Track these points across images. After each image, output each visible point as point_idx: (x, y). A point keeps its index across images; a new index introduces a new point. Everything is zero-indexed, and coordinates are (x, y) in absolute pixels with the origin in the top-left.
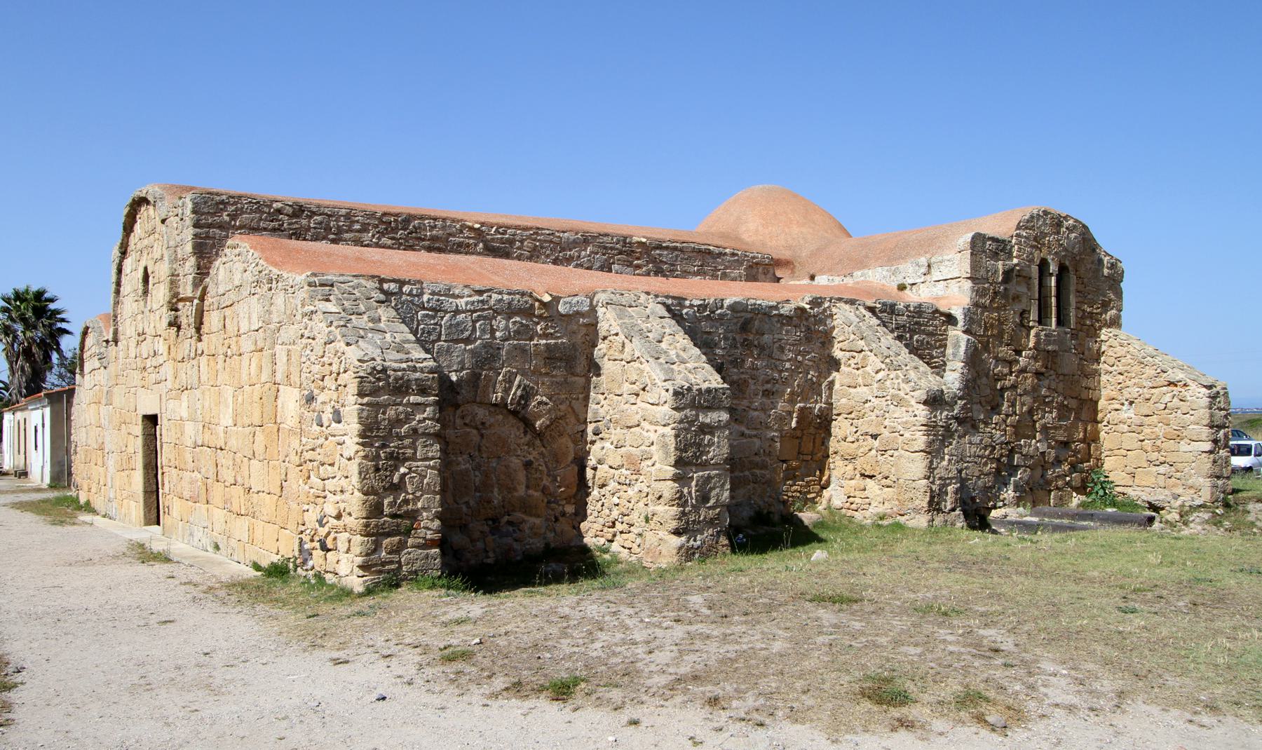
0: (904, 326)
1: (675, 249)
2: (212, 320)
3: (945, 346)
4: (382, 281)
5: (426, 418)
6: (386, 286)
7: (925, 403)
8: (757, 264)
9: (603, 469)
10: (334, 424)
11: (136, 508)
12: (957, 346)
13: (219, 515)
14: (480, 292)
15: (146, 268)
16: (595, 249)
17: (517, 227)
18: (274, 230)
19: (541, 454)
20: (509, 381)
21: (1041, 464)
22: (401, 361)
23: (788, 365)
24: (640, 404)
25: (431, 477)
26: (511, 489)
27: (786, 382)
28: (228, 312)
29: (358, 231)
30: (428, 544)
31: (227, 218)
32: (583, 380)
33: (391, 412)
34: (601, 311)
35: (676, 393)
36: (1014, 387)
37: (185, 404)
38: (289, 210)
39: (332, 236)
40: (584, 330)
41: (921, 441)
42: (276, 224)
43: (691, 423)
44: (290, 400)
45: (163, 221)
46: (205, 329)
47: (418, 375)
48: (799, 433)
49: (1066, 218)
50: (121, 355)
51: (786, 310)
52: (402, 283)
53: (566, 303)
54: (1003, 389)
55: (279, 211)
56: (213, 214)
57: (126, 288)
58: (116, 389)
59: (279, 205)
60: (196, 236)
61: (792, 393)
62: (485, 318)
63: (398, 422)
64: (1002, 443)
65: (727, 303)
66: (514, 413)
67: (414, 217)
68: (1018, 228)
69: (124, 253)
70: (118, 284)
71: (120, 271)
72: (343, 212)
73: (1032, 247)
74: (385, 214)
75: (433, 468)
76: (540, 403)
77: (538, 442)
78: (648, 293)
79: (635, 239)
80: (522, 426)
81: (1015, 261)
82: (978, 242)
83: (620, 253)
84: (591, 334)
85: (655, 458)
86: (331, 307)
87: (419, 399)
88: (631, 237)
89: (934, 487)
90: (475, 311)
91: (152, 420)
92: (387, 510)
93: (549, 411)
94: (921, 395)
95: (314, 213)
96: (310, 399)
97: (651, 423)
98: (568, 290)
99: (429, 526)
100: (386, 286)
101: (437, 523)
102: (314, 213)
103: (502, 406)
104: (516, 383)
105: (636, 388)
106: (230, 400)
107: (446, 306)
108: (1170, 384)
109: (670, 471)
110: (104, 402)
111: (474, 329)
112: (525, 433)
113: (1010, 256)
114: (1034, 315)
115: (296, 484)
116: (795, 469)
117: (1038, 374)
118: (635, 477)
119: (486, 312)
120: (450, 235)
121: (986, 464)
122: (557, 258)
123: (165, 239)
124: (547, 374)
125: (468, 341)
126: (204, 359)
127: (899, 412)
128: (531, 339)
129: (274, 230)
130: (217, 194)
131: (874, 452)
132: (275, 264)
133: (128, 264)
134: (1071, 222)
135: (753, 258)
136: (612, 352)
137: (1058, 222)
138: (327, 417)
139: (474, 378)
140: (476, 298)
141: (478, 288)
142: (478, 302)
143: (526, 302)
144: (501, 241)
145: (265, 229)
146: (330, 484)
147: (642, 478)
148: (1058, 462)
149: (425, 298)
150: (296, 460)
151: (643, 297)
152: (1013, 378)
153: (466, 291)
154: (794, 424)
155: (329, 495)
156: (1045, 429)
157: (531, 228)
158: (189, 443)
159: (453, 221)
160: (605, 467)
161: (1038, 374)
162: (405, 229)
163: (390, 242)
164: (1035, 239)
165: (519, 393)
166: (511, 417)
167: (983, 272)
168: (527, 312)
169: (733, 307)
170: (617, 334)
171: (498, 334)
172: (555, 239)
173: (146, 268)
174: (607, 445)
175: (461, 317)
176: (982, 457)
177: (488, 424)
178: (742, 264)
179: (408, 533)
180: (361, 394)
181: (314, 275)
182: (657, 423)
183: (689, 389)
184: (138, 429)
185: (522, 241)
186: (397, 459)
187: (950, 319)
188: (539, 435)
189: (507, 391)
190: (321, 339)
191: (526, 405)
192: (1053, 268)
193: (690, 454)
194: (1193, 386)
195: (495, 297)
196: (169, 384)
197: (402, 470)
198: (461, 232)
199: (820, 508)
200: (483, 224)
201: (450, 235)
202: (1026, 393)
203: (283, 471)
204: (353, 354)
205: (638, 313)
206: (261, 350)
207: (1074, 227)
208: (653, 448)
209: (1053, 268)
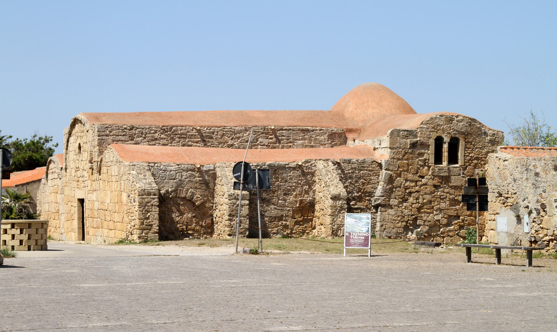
0: (355, 168)
1: (290, 130)
2: (104, 169)
3: (379, 175)
4: (150, 163)
5: (156, 202)
6: (150, 164)
7: (331, 198)
8: (334, 133)
11: (75, 235)
12: (382, 176)
13: (106, 231)
14: (178, 165)
15: (80, 144)
17: (216, 127)
18: (124, 135)
19: (199, 213)
20: (188, 190)
21: (436, 225)
23: (294, 184)
25: (157, 216)
27: (294, 191)
29: (153, 133)
30: (156, 233)
33: (146, 200)
34: (217, 169)
35: (229, 195)
36: (417, 191)
37: (95, 196)
38: (129, 128)
41: (329, 211)
42: (124, 133)
43: (235, 204)
44: (125, 196)
45: (87, 131)
46: (102, 172)
48: (301, 209)
49: (457, 117)
51: (293, 165)
52: (155, 163)
54: (410, 193)
55: (125, 128)
56: (104, 132)
57: (71, 148)
58: (66, 188)
59: (125, 126)
60: (99, 139)
61: (296, 195)
63: (148, 202)
64: (409, 215)
65: (267, 164)
66: (189, 200)
68: (422, 123)
69: (70, 134)
70: (67, 146)
71: (68, 141)
72: (148, 127)
73: (431, 132)
74: (163, 126)
79: (269, 127)
81: (418, 139)
82: (395, 134)
83: (263, 133)
84: (214, 176)
86: (134, 172)
87: (154, 197)
88: (268, 126)
89: (334, 227)
91: (82, 201)
92: (145, 224)
93: (201, 200)
94: (329, 196)
95: (137, 128)
96: (129, 196)
98: (207, 163)
99: (155, 228)
100: (150, 164)
101: (157, 228)
102: (137, 128)
103: (185, 198)
107: (168, 169)
109: (227, 217)
110: (59, 192)
113: (416, 136)
114: (432, 160)
115: (126, 219)
116: (301, 221)
117: (435, 186)
119: (180, 170)
121: (398, 223)
122: (233, 138)
123: (87, 137)
124: (200, 189)
125: (174, 179)
126: (101, 181)
129: (124, 135)
130: (106, 125)
132: (121, 157)
133: (72, 139)
134: (460, 118)
135: (332, 131)
137: (450, 120)
138: (132, 201)
139: (175, 191)
140: (177, 166)
141: (178, 163)
144: (209, 133)
148: (448, 224)
149: (162, 167)
150: (126, 212)
152: (417, 188)
153: (174, 165)
154: (298, 205)
156: (441, 210)
158: (96, 209)
159: (190, 126)
161: (435, 186)
163: (165, 137)
164: (433, 128)
167: (398, 145)
168: (193, 170)
169: (269, 165)
173: (80, 144)
175: (172, 172)
176: (396, 220)
178: (326, 134)
179: (150, 230)
180: (139, 196)
183: (234, 194)
184: (76, 204)
185: (218, 132)
187: (380, 165)
188: (198, 207)
189: (186, 193)
190: (131, 181)
191: (192, 199)
192: (447, 139)
193: (234, 213)
195: (183, 166)
196: (89, 188)
199: (310, 236)
200: (201, 127)
201: (188, 132)
202: (426, 194)
207: (462, 120)
209: (447, 139)
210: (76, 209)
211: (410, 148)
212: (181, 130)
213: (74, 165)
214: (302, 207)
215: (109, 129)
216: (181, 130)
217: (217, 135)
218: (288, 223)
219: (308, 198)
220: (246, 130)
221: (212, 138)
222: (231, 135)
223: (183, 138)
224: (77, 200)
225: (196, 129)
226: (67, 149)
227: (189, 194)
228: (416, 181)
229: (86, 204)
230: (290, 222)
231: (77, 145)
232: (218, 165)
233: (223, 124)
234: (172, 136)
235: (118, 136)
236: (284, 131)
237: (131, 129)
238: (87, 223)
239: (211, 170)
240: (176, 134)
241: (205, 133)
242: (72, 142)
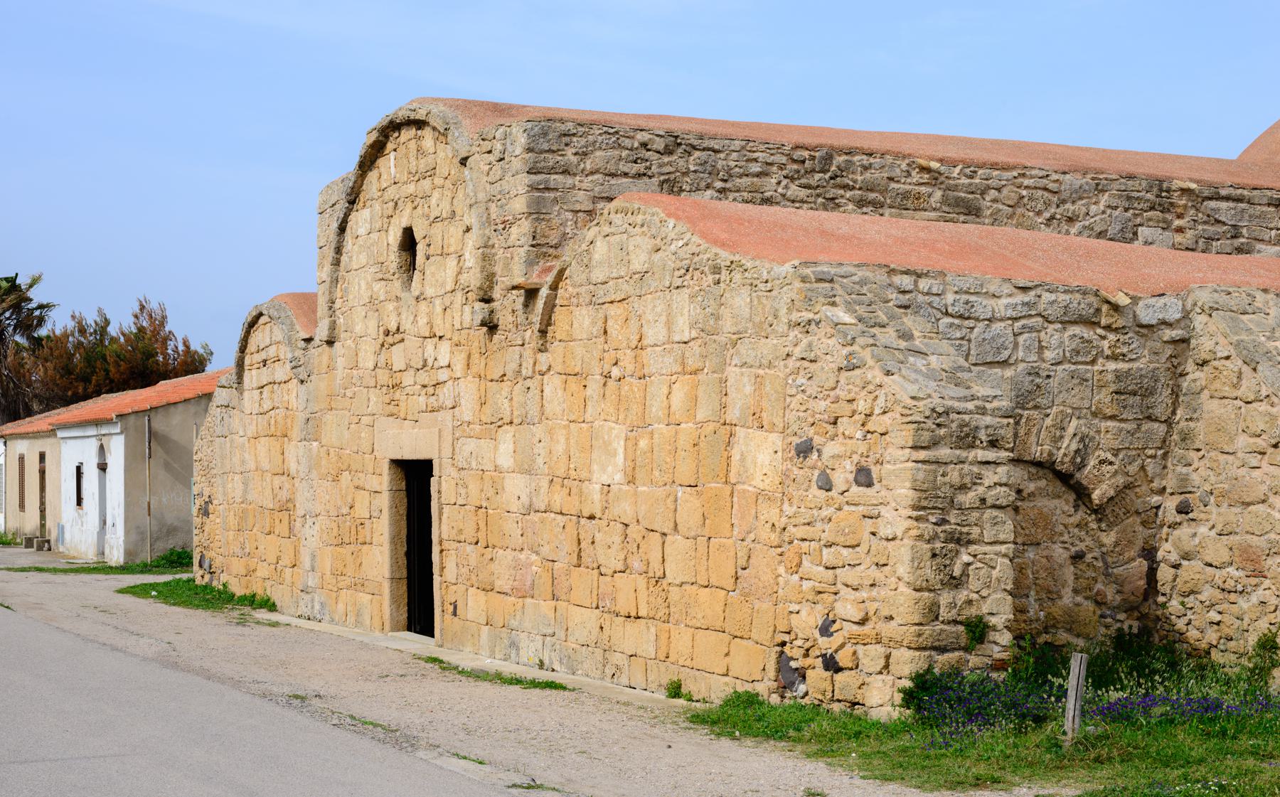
1: (1239, 200)
4: (892, 272)
6: (897, 280)
9: (1191, 570)
10: (855, 489)
14: (1024, 289)
16: (1114, 202)
17: (994, 166)
18: (639, 175)
22: (965, 399)
24: (1266, 467)
25: (1003, 570)
26: (1052, 595)
28: (613, 310)
29: (758, 175)
31: (574, 159)
32: (1163, 428)
33: (954, 475)
34: (1199, 321)
38: (659, 144)
39: (719, 185)
40: (1169, 351)
42: (640, 167)
45: (463, 162)
47: (988, 420)
50: (341, 362)
53: (1148, 306)
57: (354, 253)
58: (329, 417)
59: (642, 137)
60: (533, 188)
62: (1031, 329)
63: (963, 488)
67: (841, 151)
70: (339, 250)
72: (737, 144)
74: (797, 147)
75: (1005, 555)
76: (1102, 462)
78: (1265, 291)
79: (1177, 184)
80: (1072, 497)
87: (991, 455)
88: (1171, 179)
92: (944, 614)
104: (1071, 430)
105: (1261, 443)
106: (619, 446)
107: (979, 311)
110: (295, 433)
111: (1016, 345)
112: (1076, 507)
118: (1254, 581)
120: (891, 179)
122: (1052, 218)
125: (1004, 363)
128: (1093, 362)
129: (639, 175)
130: (562, 121)
133: (361, 220)
136: (1217, 385)
138: (842, 476)
140: (1020, 298)
142: (1024, 304)
143: (1090, 305)
145: (626, 175)
146: (844, 575)
147: (1267, 583)
149: (950, 298)
151: (1260, 297)
155: (845, 591)
157: (1014, 168)
160: (1197, 564)
162: (823, 171)
163: (803, 193)
165: (1074, 446)
166: (1058, 483)
170: (1228, 358)
171: (1048, 355)
172: (1051, 186)
174: (1203, 530)
175: (998, 326)
177: (1025, 494)
181: (806, 264)
184: (383, 482)
186: (960, 540)
188: (1099, 511)
189: (1057, 440)
191: (1082, 466)
197: (966, 558)
198: (909, 174)
203: (742, 554)
204: (901, 388)
205: (1258, 324)
206: (695, 372)
210: (384, 501)
212: (866, 168)
213: (372, 324)
216: (866, 168)
217: (995, 201)
220: (1099, 189)
222: (1047, 204)
225: (924, 169)
226: (337, 263)
227: (1069, 445)
229: (443, 487)
231: (395, 236)
232: (1204, 297)
234: (832, 192)
236: (1224, 205)
237: (668, 151)
238: (449, 571)
239: (1169, 325)
241: (955, 188)
242: (362, 231)
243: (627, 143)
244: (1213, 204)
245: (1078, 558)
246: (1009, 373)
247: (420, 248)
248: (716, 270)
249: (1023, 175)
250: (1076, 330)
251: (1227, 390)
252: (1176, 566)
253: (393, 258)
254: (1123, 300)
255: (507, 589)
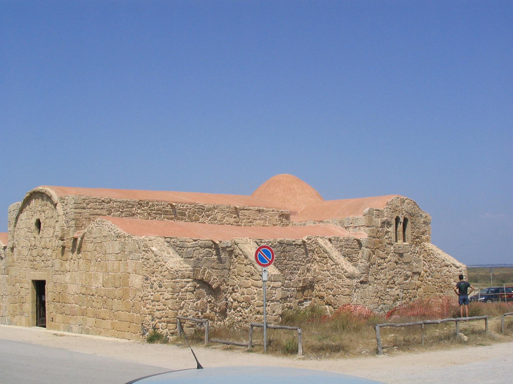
4: (166, 238)
6: (167, 239)
14: (195, 241)
16: (218, 211)
18: (102, 209)
29: (131, 208)
32: (228, 271)
33: (180, 285)
51: (299, 242)
52: (171, 238)
56: (81, 204)
59: (103, 199)
63: (182, 288)
71: (17, 218)
74: (140, 201)
77: (213, 293)
81: (385, 218)
85: (256, 299)
90: (193, 247)
97: (255, 286)
102: (115, 202)
108: (447, 266)
114: (394, 239)
125: (191, 258)
127: (340, 281)
128: (212, 256)
129: (102, 209)
131: (331, 296)
138: (156, 285)
140: (194, 243)
141: (195, 239)
145: (98, 209)
162: (147, 206)
174: (238, 294)
182: (258, 287)
194: (453, 267)
208: (256, 295)
209: (402, 220)
210: (30, 291)
211: (381, 227)
212: (157, 205)
214: (304, 287)
215: (87, 201)
218: (292, 304)
219: (309, 276)
221: (185, 215)
223: (159, 214)
224: (31, 282)
226: (15, 226)
228: (384, 258)
229: (48, 287)
230: (294, 303)
231: (34, 221)
233: (193, 201)
234: (149, 211)
235: (95, 209)
236: (246, 211)
237: (109, 202)
240: (152, 210)
241: (179, 209)
243: (99, 201)
244: (243, 211)
245: (210, 302)
246: (192, 259)
247: (42, 225)
248: (125, 237)
249: (196, 206)
250: (208, 249)
251: (242, 262)
252: (232, 303)
253: (34, 227)
254: (218, 242)
255: (69, 313)
